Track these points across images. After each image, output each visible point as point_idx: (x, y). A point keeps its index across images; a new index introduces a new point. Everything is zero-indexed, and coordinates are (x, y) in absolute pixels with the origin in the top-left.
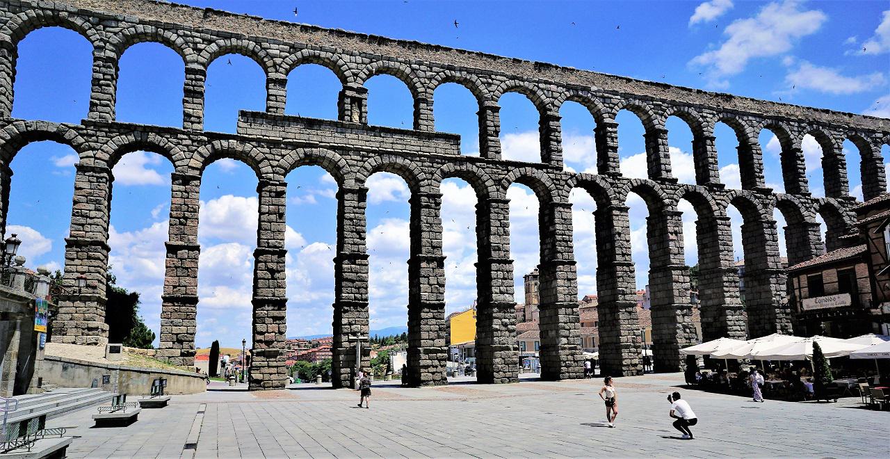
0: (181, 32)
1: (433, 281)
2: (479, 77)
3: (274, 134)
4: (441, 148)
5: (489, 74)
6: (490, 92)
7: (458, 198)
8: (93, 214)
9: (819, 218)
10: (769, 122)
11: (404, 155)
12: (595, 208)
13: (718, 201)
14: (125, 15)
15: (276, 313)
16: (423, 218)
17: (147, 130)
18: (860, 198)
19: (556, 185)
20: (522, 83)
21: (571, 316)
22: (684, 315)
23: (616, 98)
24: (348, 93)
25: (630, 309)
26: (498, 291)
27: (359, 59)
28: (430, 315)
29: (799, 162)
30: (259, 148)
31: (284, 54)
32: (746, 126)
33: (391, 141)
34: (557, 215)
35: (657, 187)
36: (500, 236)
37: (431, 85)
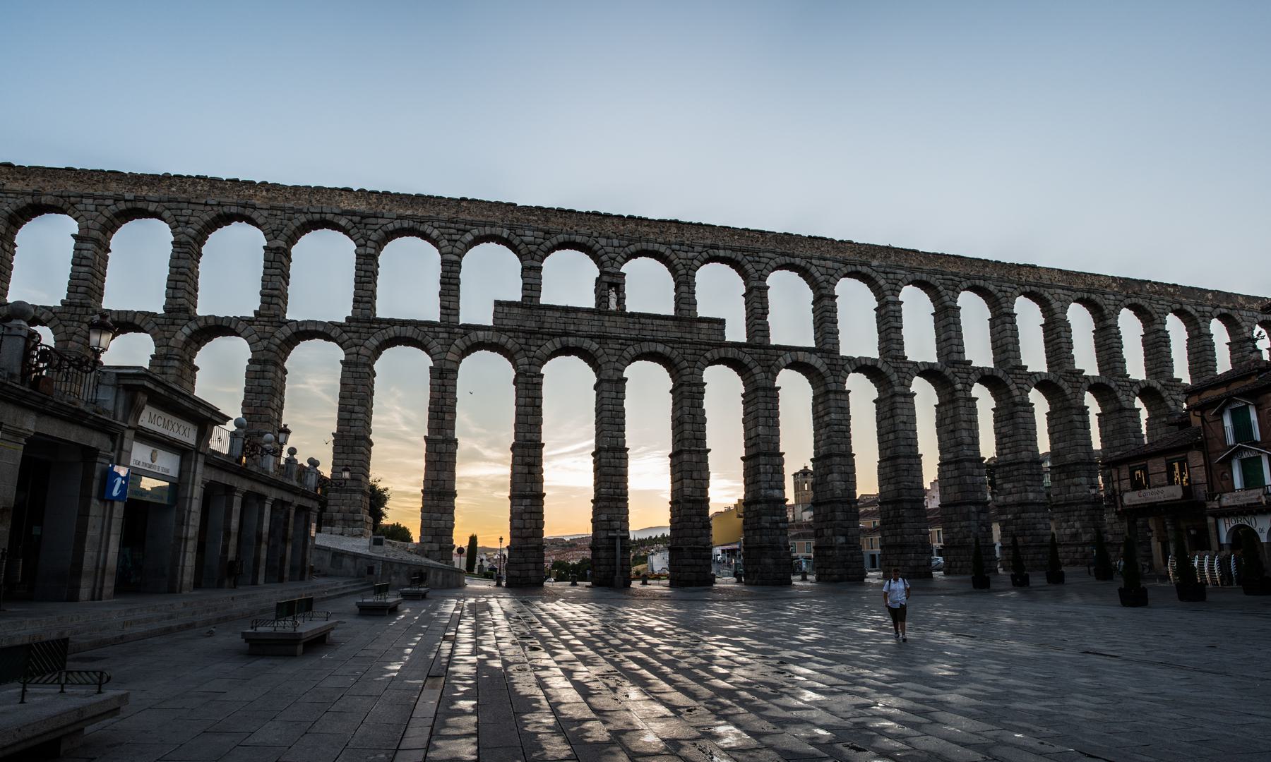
0: (436, 224)
3: (531, 324)
4: (704, 333)
5: (756, 252)
7: (723, 390)
8: (357, 409)
9: (1138, 403)
10: (1079, 295)
12: (876, 396)
15: (534, 509)
16: (686, 409)
17: (404, 323)
18: (1187, 380)
23: (901, 274)
27: (616, 242)
28: (694, 512)
31: (539, 241)
33: (651, 327)
34: (832, 403)
35: (948, 371)
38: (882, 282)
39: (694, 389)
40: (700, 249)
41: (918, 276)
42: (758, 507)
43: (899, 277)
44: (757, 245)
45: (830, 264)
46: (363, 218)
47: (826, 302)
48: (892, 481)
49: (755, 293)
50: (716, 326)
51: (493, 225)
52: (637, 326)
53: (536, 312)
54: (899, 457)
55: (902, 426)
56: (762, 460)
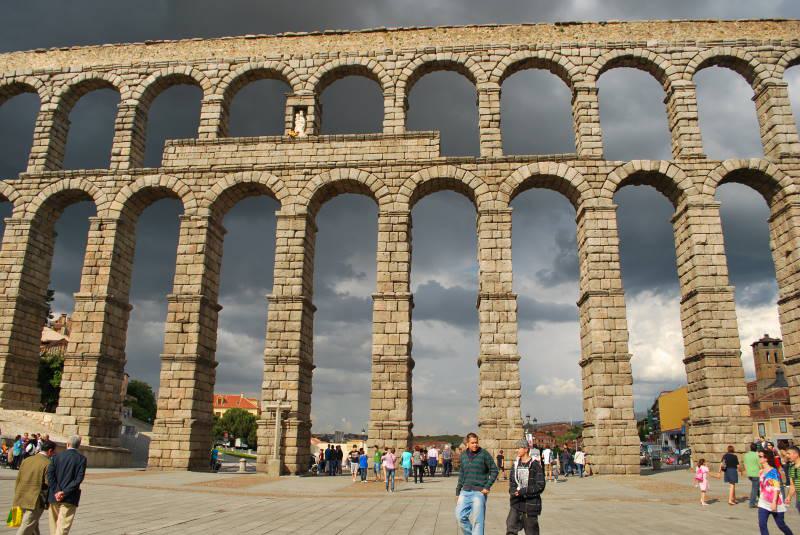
1: (389, 328)
2: (470, 56)
3: (203, 163)
14: (71, 66)
15: (183, 375)
20: (534, 54)
24: (291, 102)
25: (726, 361)
28: (385, 376)
30: (185, 181)
31: (222, 73)
33: (344, 151)
38: (663, 66)
39: (394, 219)
40: (411, 56)
41: (716, 51)
43: (691, 55)
44: (485, 42)
46: (51, 75)
51: (177, 64)
52: (327, 152)
53: (211, 148)
55: (697, 249)
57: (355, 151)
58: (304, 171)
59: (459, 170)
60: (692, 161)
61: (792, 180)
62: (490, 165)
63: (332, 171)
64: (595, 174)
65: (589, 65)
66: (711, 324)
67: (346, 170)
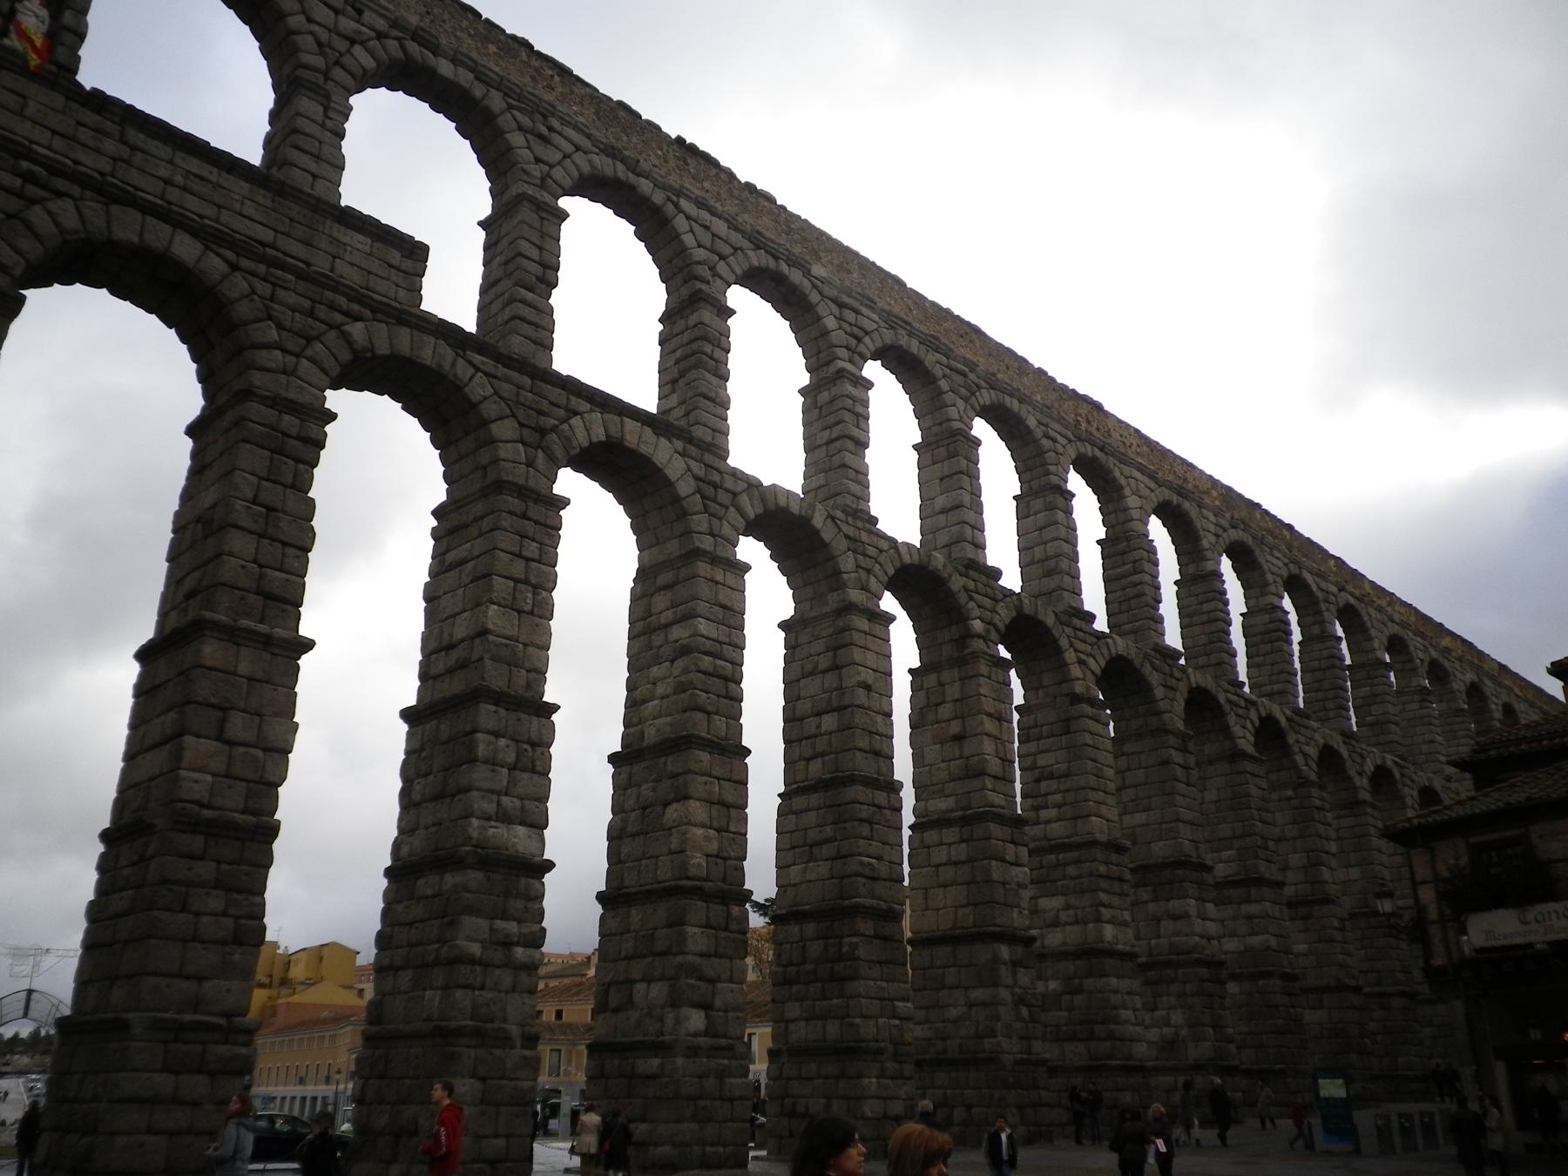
1: (238, 726)
5: (545, 113)
6: (538, 160)
11: (212, 238)
13: (1083, 657)
16: (245, 483)
19: (703, 497)
20: (632, 178)
21: (723, 934)
22: (1016, 964)
26: (490, 807)
28: (206, 870)
29: (1220, 605)
32: (1127, 492)
36: (519, 612)
37: (347, 60)
39: (289, 422)
40: (381, 24)
42: (451, 879)
44: (549, 97)
45: (720, 227)
47: (707, 315)
48: (826, 850)
49: (526, 213)
50: (395, 256)
52: (110, 146)
54: (852, 780)
55: (861, 696)
56: (487, 715)
57: (196, 186)
58: (24, 164)
59: (460, 360)
60: (860, 524)
61: (977, 612)
62: (527, 381)
63: (115, 210)
64: (716, 486)
65: (722, 257)
66: (871, 851)
67: (166, 229)
